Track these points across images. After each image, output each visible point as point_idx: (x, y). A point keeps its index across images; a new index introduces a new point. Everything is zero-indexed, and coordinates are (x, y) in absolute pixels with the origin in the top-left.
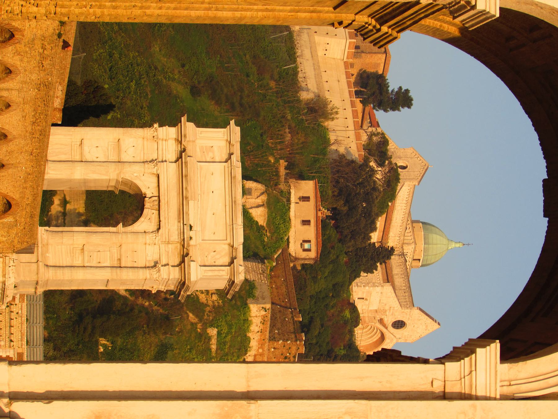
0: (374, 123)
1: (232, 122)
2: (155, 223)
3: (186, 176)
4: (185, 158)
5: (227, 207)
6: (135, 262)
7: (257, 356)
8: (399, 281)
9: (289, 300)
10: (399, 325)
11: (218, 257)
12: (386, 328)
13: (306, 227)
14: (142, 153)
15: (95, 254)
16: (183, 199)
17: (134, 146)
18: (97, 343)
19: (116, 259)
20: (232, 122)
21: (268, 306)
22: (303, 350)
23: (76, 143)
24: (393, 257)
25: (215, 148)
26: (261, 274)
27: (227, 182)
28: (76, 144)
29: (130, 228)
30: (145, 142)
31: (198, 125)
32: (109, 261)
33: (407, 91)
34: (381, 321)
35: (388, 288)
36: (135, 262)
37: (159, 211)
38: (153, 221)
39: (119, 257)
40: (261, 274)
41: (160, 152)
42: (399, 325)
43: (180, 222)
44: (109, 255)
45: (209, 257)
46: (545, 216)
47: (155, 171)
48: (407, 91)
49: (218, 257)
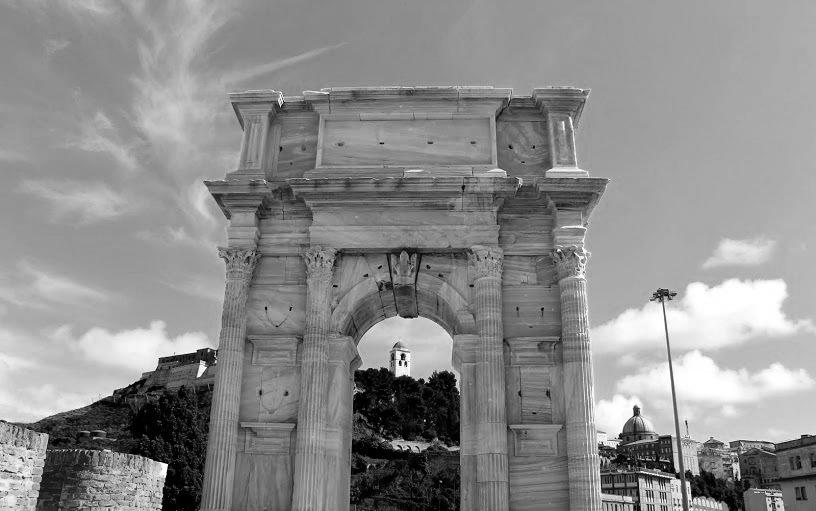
2: (452, 264)
3: (348, 183)
4: (306, 184)
6: (542, 309)
11: (523, 141)
14: (281, 289)
15: (526, 402)
16: (399, 191)
19: (539, 354)
23: (247, 443)
25: (285, 142)
27: (364, 115)
30: (259, 281)
32: (545, 370)
36: (542, 309)
39: (536, 347)
41: (285, 250)
45: (524, 156)
47: (328, 257)
49: (523, 141)
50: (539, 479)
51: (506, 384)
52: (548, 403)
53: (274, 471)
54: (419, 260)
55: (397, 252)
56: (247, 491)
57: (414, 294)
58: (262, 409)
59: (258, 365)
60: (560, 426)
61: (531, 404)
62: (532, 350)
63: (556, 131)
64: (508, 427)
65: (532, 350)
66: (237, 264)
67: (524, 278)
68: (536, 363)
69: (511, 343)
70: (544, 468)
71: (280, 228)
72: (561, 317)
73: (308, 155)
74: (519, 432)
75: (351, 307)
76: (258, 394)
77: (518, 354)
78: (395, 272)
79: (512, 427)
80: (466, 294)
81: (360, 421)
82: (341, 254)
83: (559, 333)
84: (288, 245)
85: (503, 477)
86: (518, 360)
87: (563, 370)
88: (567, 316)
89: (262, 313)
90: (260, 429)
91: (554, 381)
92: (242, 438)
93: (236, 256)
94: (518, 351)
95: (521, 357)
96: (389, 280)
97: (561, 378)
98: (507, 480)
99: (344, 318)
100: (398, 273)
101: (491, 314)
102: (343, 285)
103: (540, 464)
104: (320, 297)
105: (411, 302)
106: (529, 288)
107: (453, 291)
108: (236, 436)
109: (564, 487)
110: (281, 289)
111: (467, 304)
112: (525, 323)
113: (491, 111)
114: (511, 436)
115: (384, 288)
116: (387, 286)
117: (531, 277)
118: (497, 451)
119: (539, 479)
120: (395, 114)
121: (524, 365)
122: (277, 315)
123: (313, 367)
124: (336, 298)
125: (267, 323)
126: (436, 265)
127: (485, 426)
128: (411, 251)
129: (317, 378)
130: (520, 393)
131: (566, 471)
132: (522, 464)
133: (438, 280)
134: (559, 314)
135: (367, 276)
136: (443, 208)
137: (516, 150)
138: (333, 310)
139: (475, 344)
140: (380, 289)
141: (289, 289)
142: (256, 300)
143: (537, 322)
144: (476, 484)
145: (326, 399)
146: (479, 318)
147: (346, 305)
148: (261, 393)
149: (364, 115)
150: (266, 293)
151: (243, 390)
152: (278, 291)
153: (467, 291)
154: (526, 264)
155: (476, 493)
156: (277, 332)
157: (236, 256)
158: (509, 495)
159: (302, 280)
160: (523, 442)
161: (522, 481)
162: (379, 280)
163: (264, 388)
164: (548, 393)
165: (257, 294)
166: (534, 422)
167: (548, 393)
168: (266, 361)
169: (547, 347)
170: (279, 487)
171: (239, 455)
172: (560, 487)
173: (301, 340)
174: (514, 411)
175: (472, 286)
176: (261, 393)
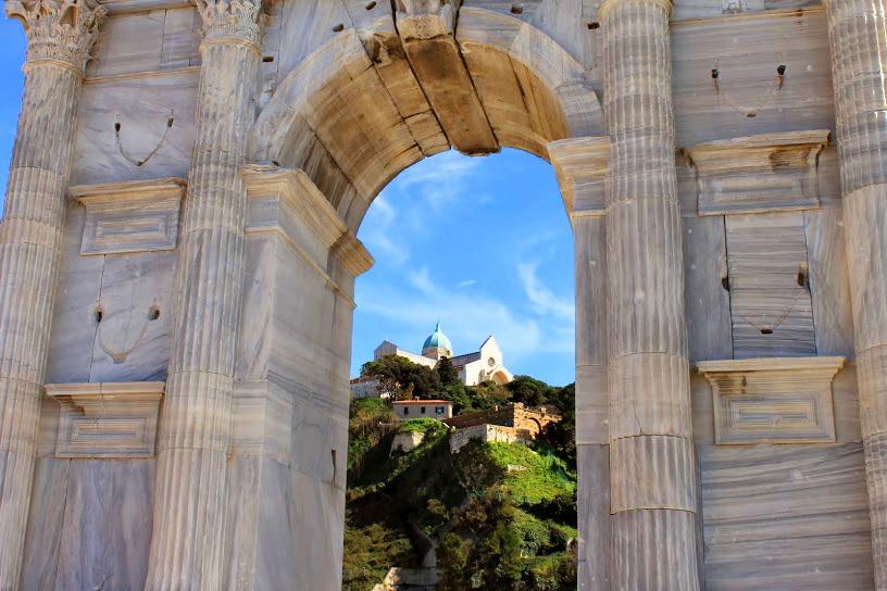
6: (781, 70)
10: (492, 361)
14: (151, 81)
15: (742, 302)
17: (118, 127)
18: (523, 560)
19: (772, 180)
21: (488, 426)
23: (62, 435)
28: (71, 429)
30: (104, 70)
32: (793, 219)
35: (468, 367)
36: (781, 70)
39: (766, 162)
42: (492, 361)
44: (748, 222)
50: (783, 505)
51: (688, 259)
52: (802, 304)
53: (119, 495)
56: (56, 548)
57: (459, 67)
58: (98, 353)
59: (94, 252)
60: (841, 359)
61: (754, 305)
62: (760, 171)
64: (694, 372)
65: (760, 171)
66: (44, 28)
68: (768, 203)
69: (698, 156)
70: (797, 475)
72: (830, 84)
74: (724, 380)
75: (301, 105)
76: (91, 318)
77: (719, 184)
78: (403, 10)
79: (705, 366)
80: (579, 46)
81: (554, 468)
83: (830, 123)
85: (678, 498)
86: (719, 197)
87: (840, 216)
88: (843, 75)
89: (109, 138)
90: (90, 399)
91: (818, 243)
92: (51, 422)
93: (42, 10)
94: (721, 175)
95: (726, 191)
96: (389, 33)
97: (838, 238)
98: (693, 509)
99: (284, 128)
100: (408, 9)
101: (642, 83)
102: (283, 57)
103: (785, 465)
104: (224, 82)
105: (464, 101)
106: (744, 21)
107: (546, 40)
108: (36, 417)
109: (858, 524)
110: (151, 81)
111: (581, 70)
112: (737, 105)
114: (705, 393)
115: (384, 56)
116: (390, 52)
118: (660, 427)
119: (783, 505)
121: (736, 208)
122: (140, 138)
123: (200, 239)
124: (266, 87)
125: (122, 160)
129: (208, 271)
130: (726, 283)
131: (860, 483)
132: (735, 464)
133: (513, 20)
134: (826, 80)
135: (340, 28)
138: (258, 112)
139: (603, 162)
140: (375, 60)
141: (167, 80)
142: (97, 110)
143: (766, 102)
144: (609, 517)
145: (236, 318)
146: (609, 98)
147: (289, 98)
148: (100, 316)
150: (119, 94)
151: (58, 310)
152: (144, 87)
153: (580, 40)
155: (608, 542)
156: (140, 170)
157: (42, 10)
158: (702, 548)
160: (735, 407)
161: (733, 511)
162: (368, 34)
163: (107, 308)
164: (803, 279)
165: (99, 97)
166: (769, 351)
167: (803, 279)
168: (111, 244)
169: (795, 159)
170: (128, 536)
171: (45, 464)
172: (839, 524)
173: (183, 185)
174: (711, 329)
175: (593, 26)
176: (100, 316)
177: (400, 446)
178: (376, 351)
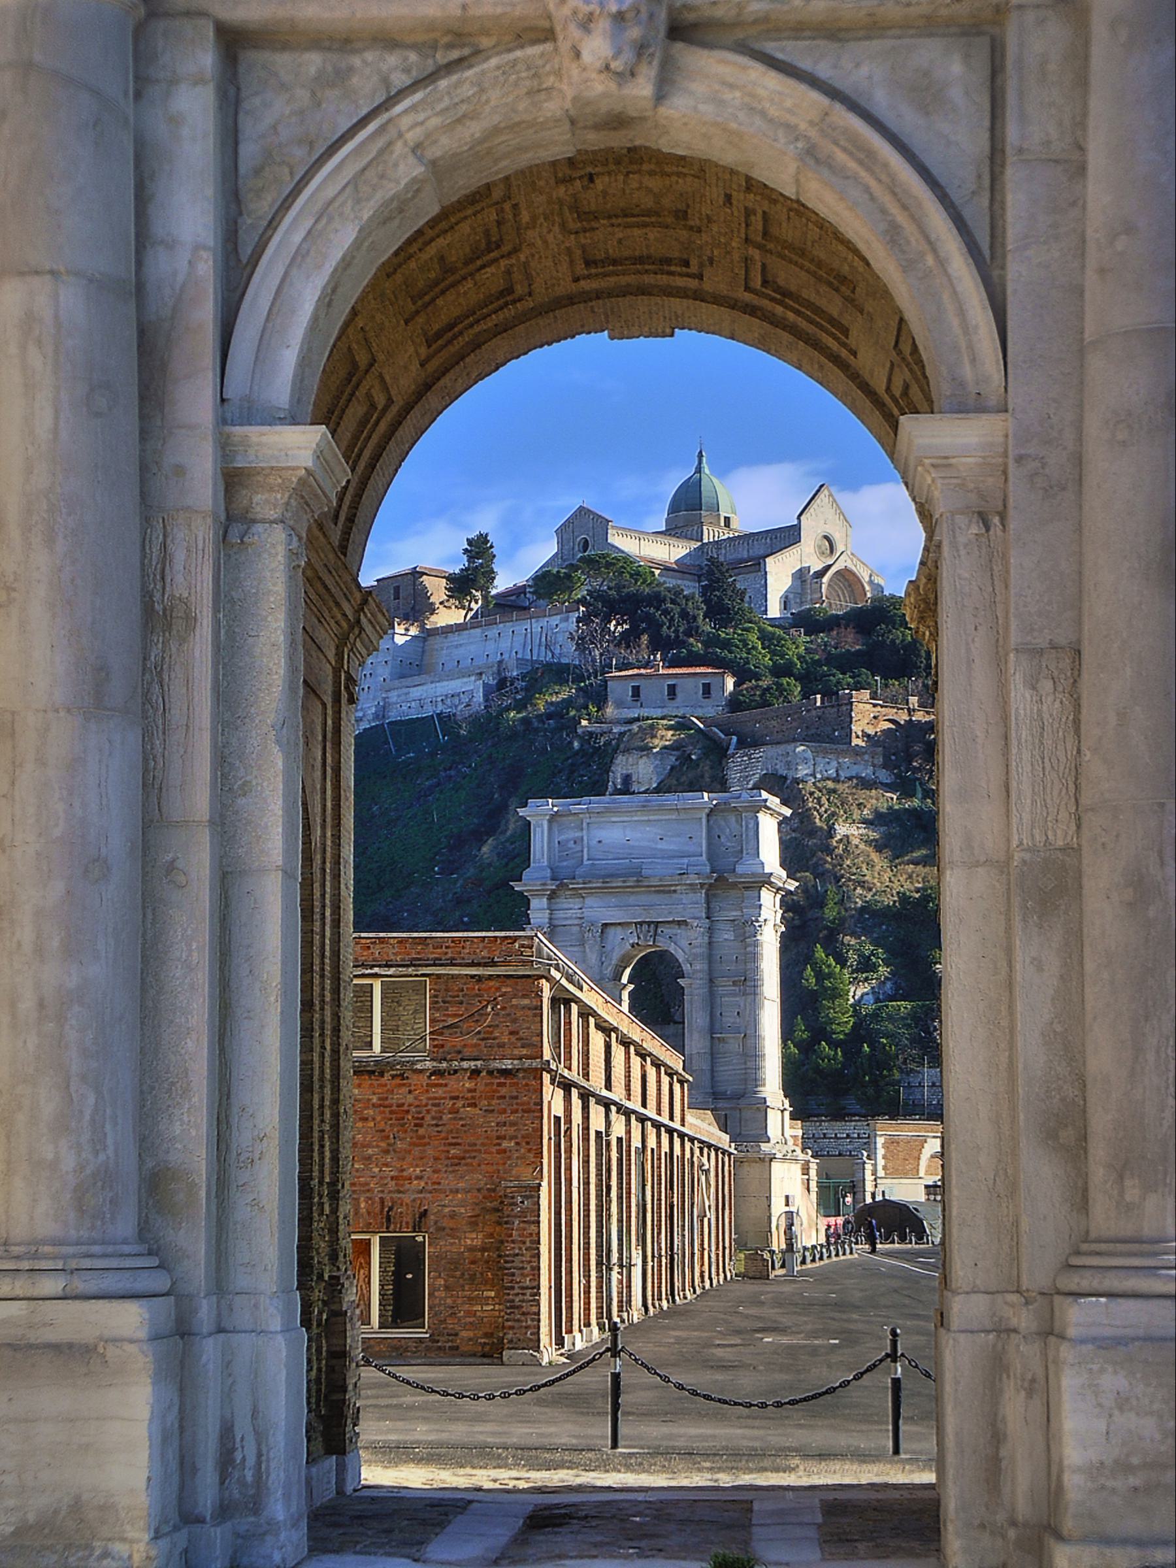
0: (518, 591)
1: (522, 812)
5: (652, 818)
7: (876, 762)
8: (758, 550)
9: (789, 715)
12: (829, 566)
13: (678, 690)
20: (522, 812)
22: (865, 694)
24: (722, 559)
25: (562, 838)
26: (750, 759)
29: (686, 967)
31: (527, 863)
33: (470, 542)
34: (821, 574)
37: (657, 924)
38: (674, 931)
40: (750, 759)
43: (675, 891)
46: (672, 335)
48: (470, 542)
51: (712, 1008)
54: (657, 927)
55: (641, 923)
63: (747, 826)
64: (712, 1038)
67: (726, 936)
71: (565, 906)
73: (579, 848)
80: (686, 950)
82: (605, 925)
84: (571, 918)
102: (608, 948)
113: (704, 816)
117: (730, 936)
120: (636, 818)
121: (724, 995)
126: (668, 930)
127: (696, 1036)
128: (649, 923)
136: (669, 892)
137: (723, 839)
141: (575, 949)
149: (614, 819)
154: (728, 926)
159: (582, 944)
177: (627, 779)
178: (560, 532)
